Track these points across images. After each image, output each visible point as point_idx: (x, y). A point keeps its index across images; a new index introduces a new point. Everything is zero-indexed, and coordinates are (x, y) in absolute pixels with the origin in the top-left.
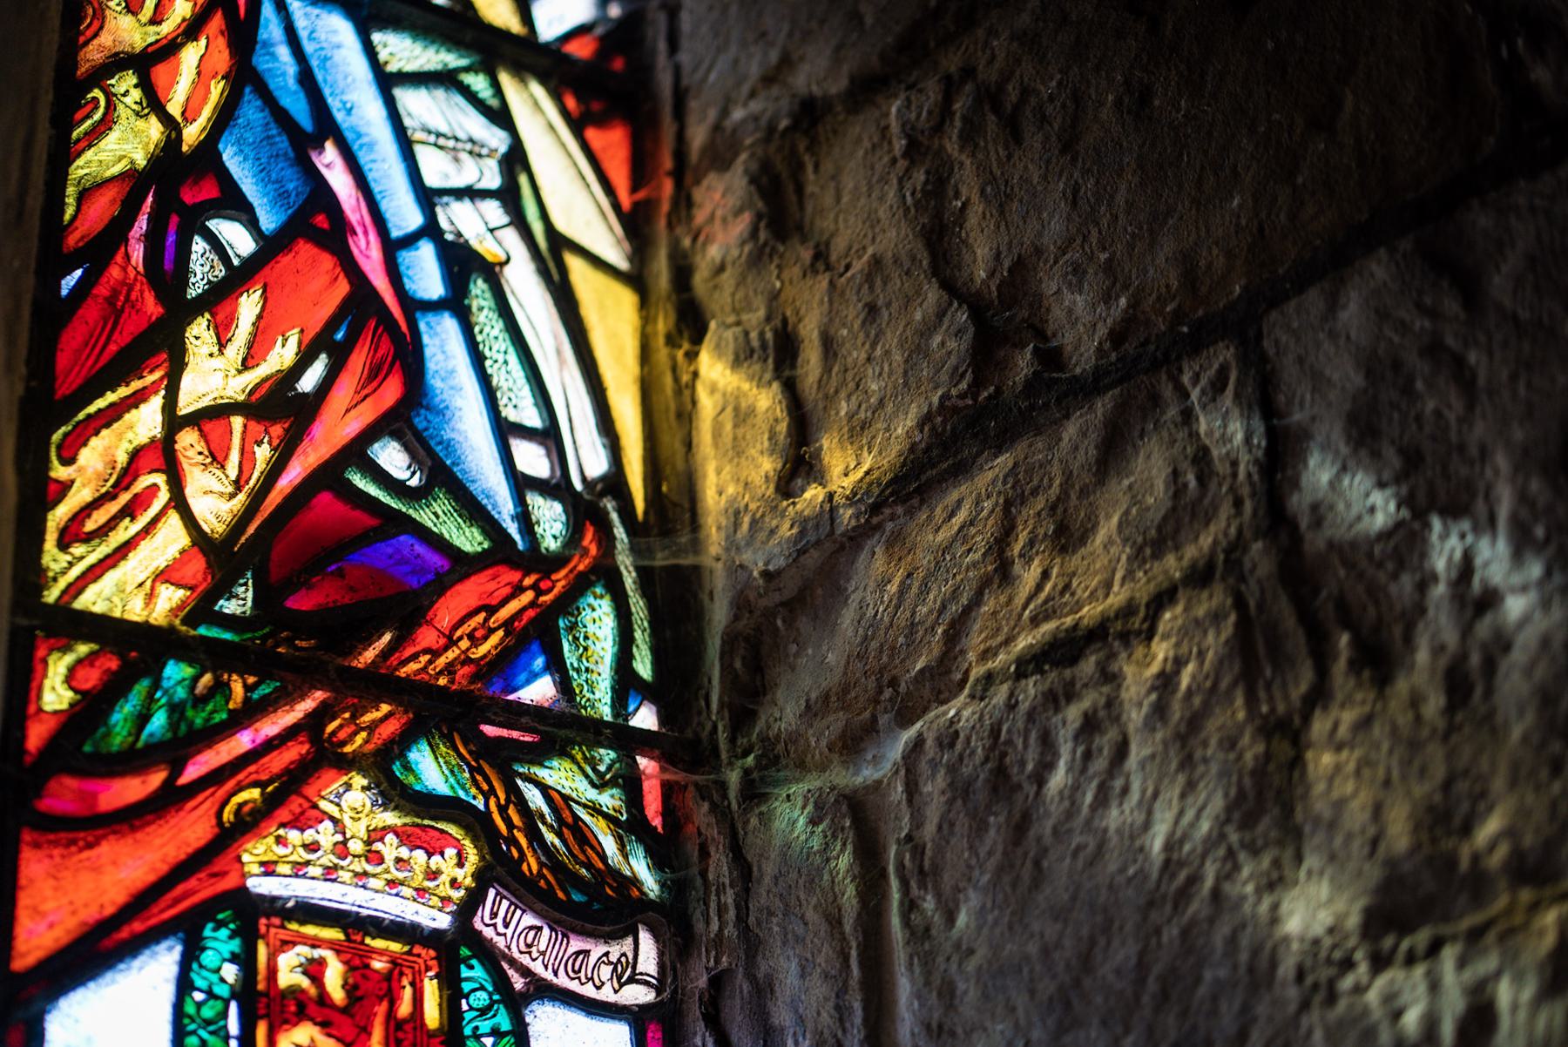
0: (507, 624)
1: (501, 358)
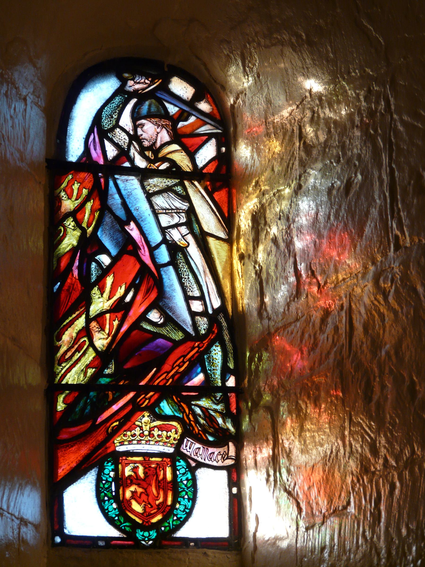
0: (189, 360)
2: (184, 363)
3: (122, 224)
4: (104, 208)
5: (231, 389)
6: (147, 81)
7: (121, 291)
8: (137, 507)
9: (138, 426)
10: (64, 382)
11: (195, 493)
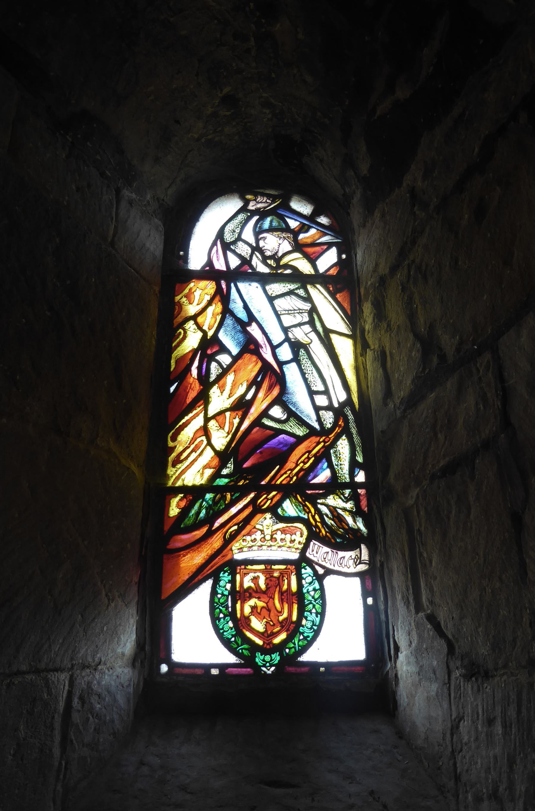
0: (315, 455)
1: (310, 372)
2: (309, 458)
4: (227, 311)
5: (361, 485)
6: (268, 201)
8: (257, 624)
11: (323, 606)
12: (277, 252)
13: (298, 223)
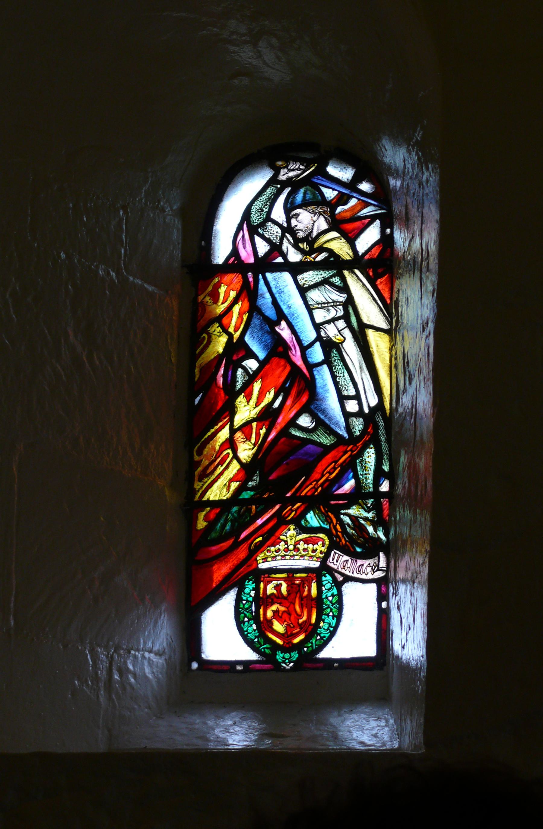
0: (341, 465)
1: (342, 375)
2: (334, 469)
3: (272, 324)
4: (254, 309)
6: (301, 167)
7: (269, 397)
8: (278, 627)
9: (283, 540)
10: (205, 498)
12: (312, 232)
13: (337, 192)
